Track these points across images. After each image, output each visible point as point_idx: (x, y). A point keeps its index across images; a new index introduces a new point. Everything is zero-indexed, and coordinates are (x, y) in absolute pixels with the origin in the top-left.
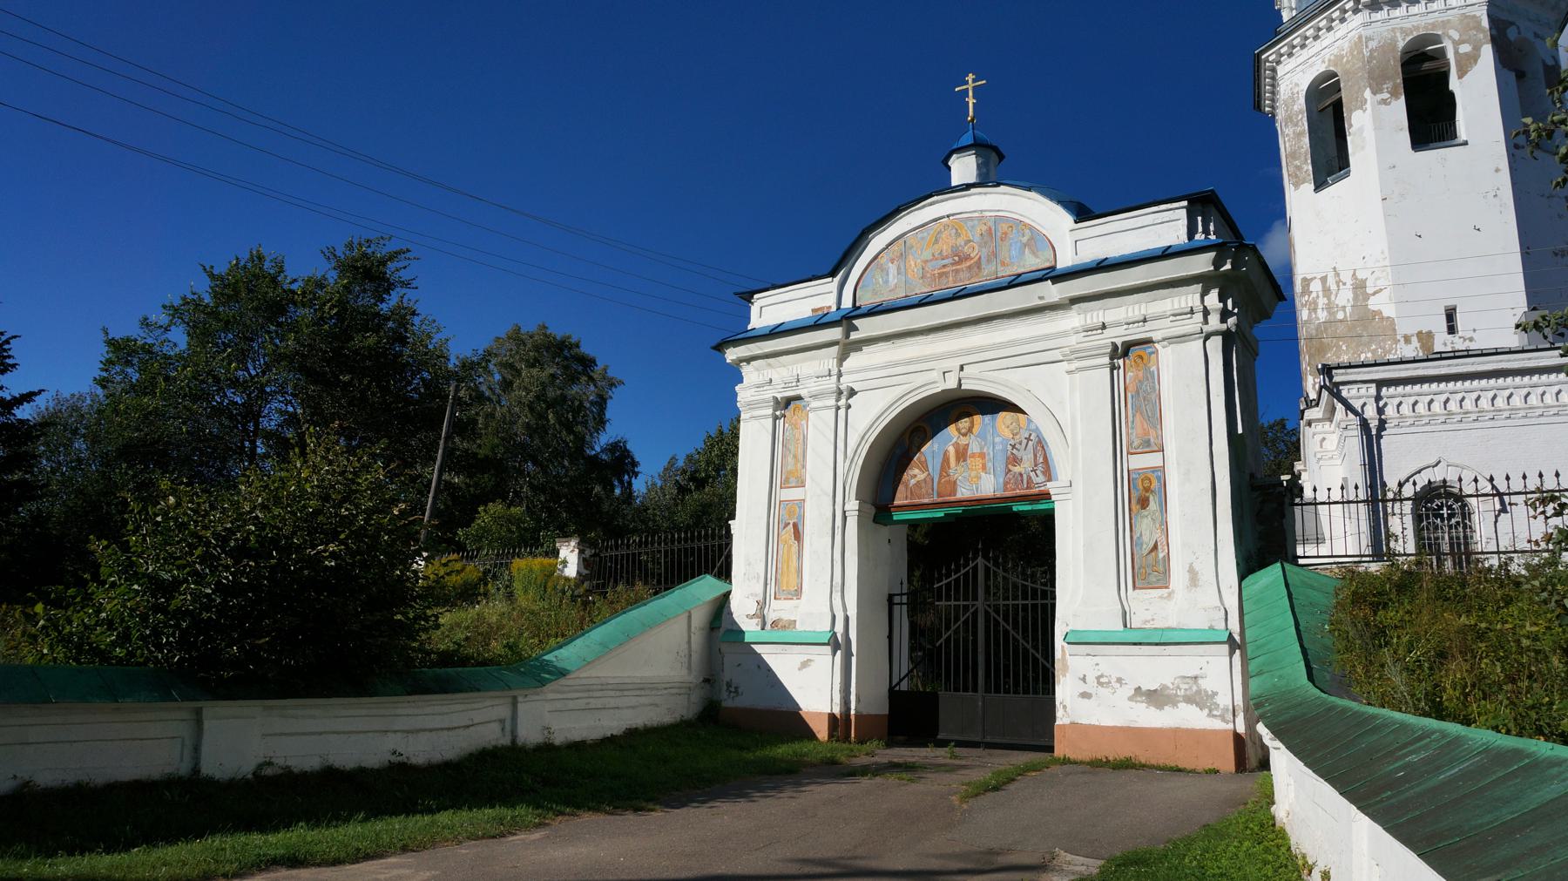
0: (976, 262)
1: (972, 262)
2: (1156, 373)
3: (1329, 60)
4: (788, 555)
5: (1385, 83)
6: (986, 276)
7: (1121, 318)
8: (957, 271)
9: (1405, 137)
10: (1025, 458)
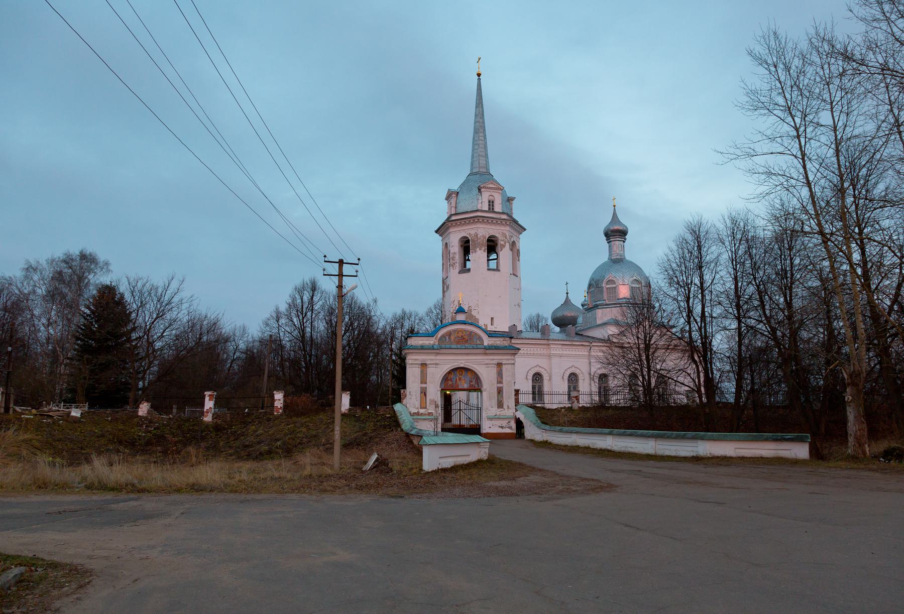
7: (497, 358)
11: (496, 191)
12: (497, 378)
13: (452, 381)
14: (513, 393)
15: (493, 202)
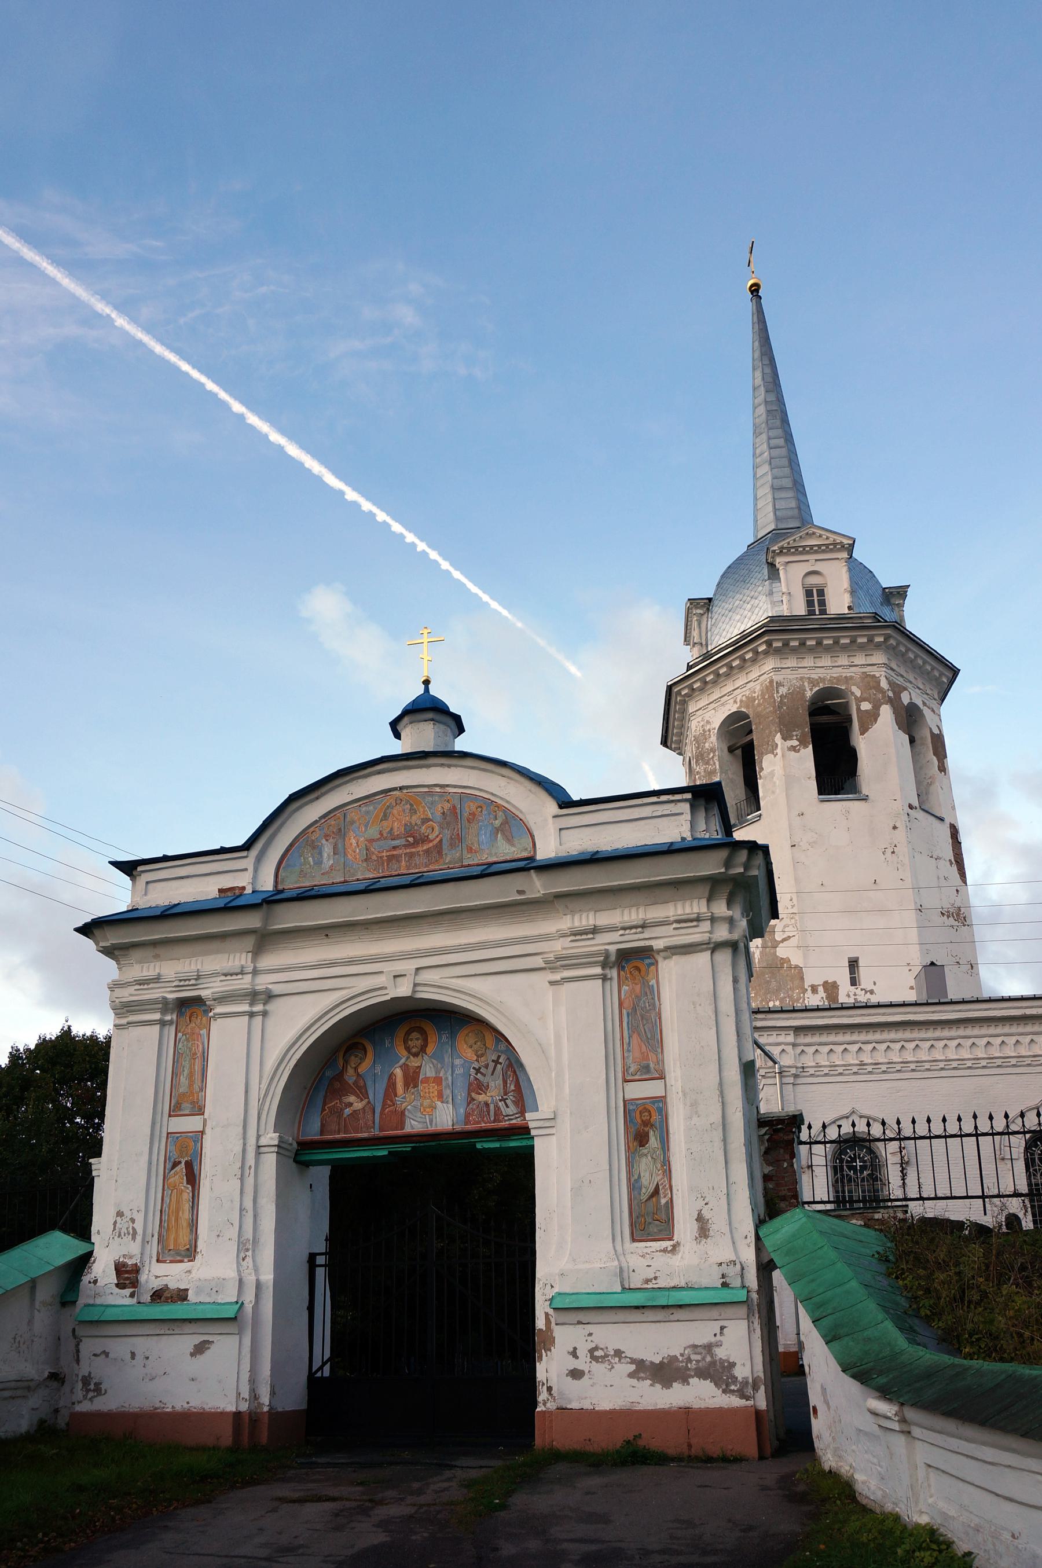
0: (436, 846)
1: (431, 845)
2: (655, 986)
3: (741, 701)
4: (178, 1202)
5: (795, 731)
6: (450, 861)
8: (411, 856)
9: (813, 785)
10: (492, 1084)
13: (362, 1092)
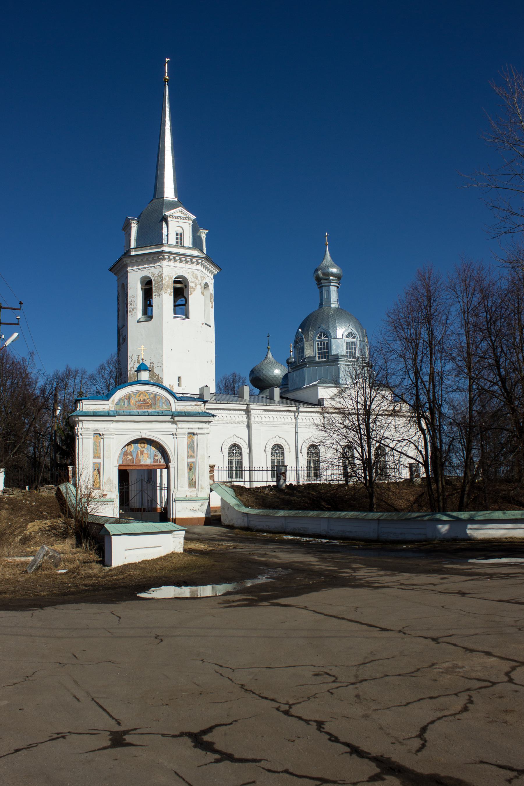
11: (185, 221)
12: (188, 452)
14: (209, 469)
15: (181, 235)
